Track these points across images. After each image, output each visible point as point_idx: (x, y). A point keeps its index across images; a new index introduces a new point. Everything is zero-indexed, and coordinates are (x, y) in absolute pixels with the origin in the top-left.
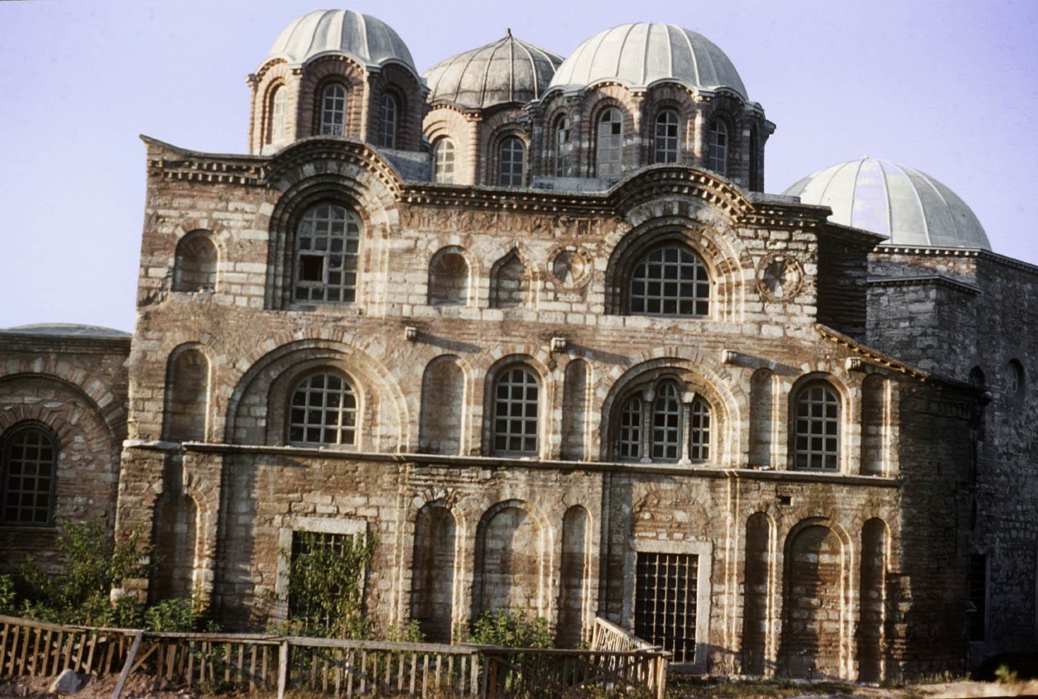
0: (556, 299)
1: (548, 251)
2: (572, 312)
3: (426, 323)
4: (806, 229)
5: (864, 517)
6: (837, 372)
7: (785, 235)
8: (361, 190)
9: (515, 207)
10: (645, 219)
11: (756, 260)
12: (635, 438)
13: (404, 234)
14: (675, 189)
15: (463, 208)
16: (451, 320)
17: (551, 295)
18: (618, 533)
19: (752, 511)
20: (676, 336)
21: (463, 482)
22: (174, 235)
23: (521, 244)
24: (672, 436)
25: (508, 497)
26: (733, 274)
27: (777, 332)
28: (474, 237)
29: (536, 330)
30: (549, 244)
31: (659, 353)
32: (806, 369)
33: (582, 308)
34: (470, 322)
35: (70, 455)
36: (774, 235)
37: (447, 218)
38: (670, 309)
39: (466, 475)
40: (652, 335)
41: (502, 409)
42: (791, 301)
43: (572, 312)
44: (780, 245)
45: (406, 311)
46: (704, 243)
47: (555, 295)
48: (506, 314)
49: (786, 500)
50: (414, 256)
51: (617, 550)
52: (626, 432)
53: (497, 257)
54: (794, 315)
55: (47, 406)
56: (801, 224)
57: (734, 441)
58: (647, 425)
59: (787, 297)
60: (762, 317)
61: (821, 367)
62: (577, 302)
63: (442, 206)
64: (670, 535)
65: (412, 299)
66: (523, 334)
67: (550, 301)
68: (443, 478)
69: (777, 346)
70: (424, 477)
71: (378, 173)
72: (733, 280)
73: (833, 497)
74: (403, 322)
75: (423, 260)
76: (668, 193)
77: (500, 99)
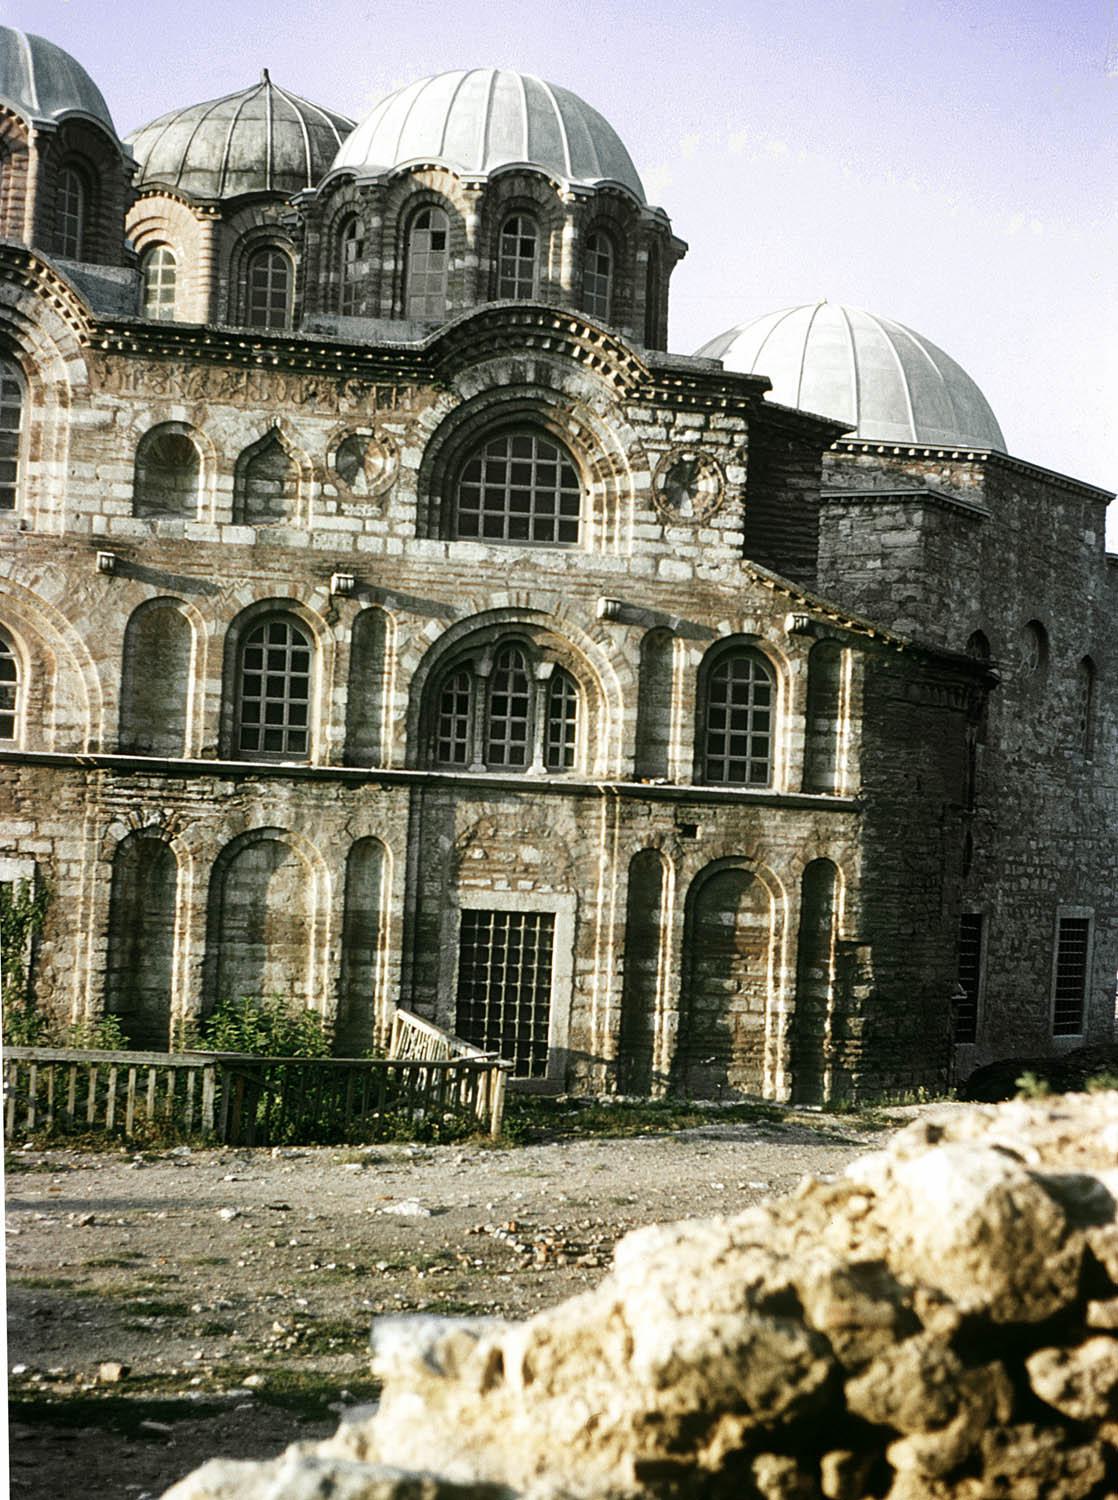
0: (340, 512)
1: (327, 433)
2: (364, 533)
3: (131, 546)
4: (731, 411)
5: (806, 857)
6: (772, 634)
7: (697, 420)
8: (24, 326)
9: (275, 362)
10: (481, 388)
11: (653, 458)
12: (461, 733)
13: (97, 401)
14: (530, 343)
15: (192, 361)
16: (171, 542)
17: (332, 506)
18: (432, 879)
19: (638, 848)
20: (528, 575)
21: (188, 800)
23: (285, 422)
24: (519, 731)
25: (261, 824)
26: (617, 479)
27: (683, 572)
28: (210, 409)
30: (329, 424)
31: (500, 600)
32: (725, 629)
33: (381, 527)
34: (202, 545)
36: (682, 419)
37: (166, 378)
38: (518, 531)
39: (195, 788)
40: (489, 573)
41: (253, 685)
42: (706, 524)
43: (364, 533)
44: (690, 436)
45: (99, 525)
46: (574, 429)
47: (339, 505)
48: (260, 535)
49: (690, 831)
50: (112, 436)
51: (431, 907)
52: (447, 723)
53: (246, 443)
54: (709, 545)
56: (724, 404)
57: (613, 739)
58: (479, 713)
59: (699, 517)
60: (661, 548)
61: (749, 626)
62: (373, 518)
63: (157, 356)
64: (512, 884)
65: (108, 508)
66: (286, 566)
67: (330, 515)
68: (157, 793)
69: (681, 594)
70: (126, 792)
71: (52, 299)
72: (618, 489)
73: (761, 827)
74: (93, 543)
75: (126, 443)
76: (519, 348)
77: (251, 186)
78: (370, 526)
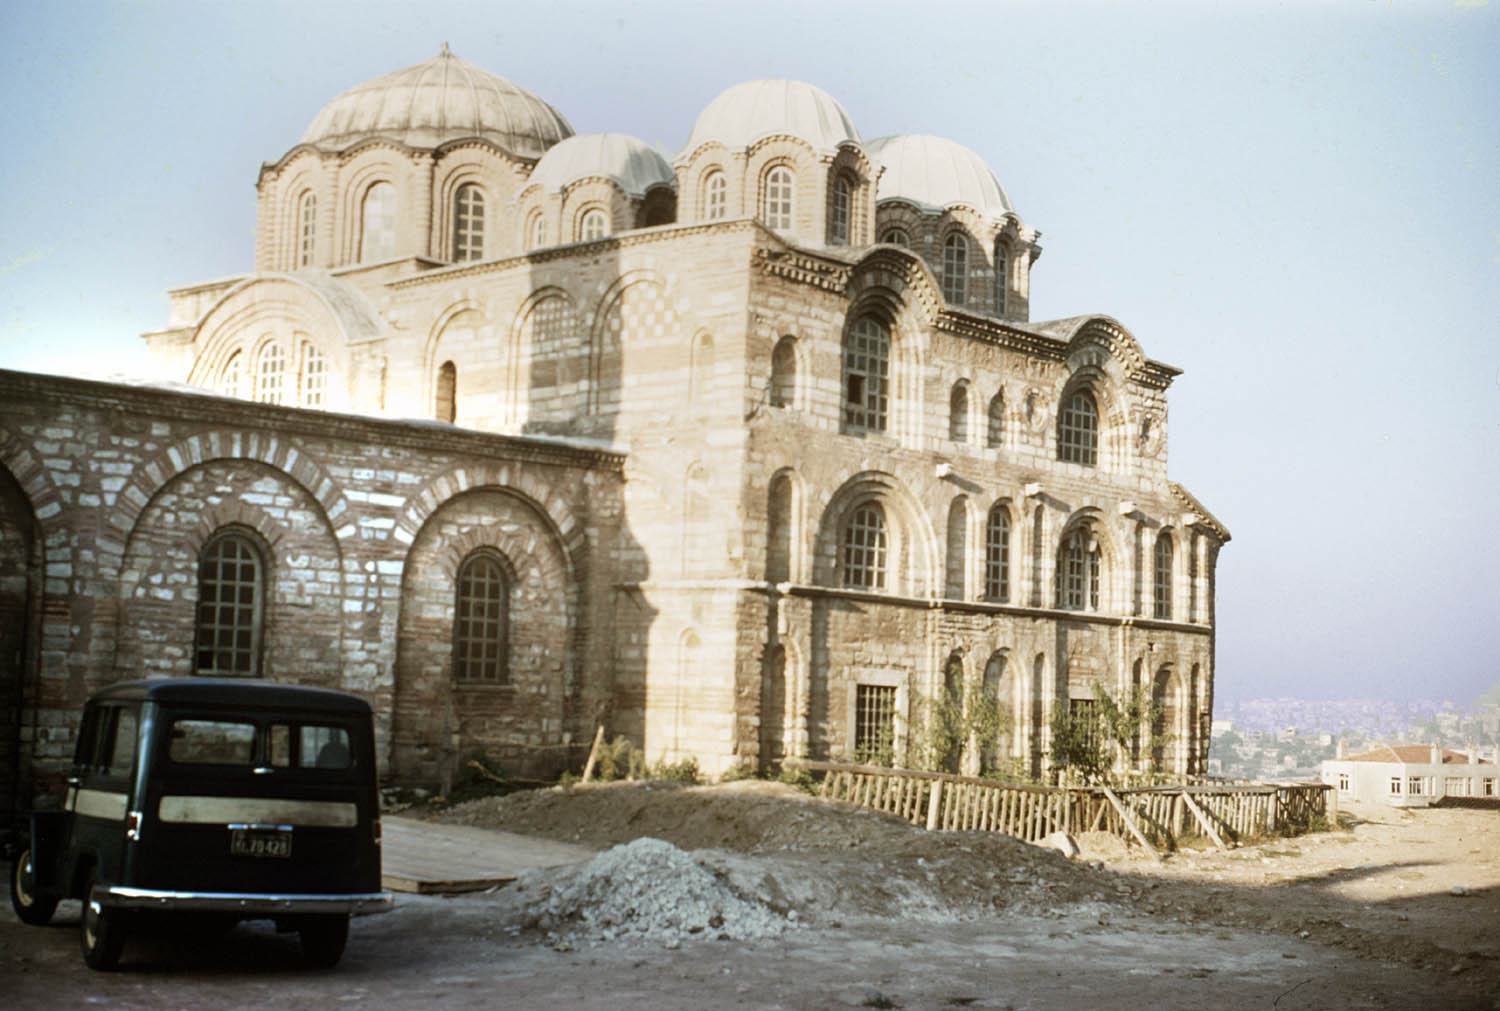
6: (1178, 527)
8: (901, 307)
22: (769, 339)
26: (1122, 428)
29: (1017, 473)
35: (526, 593)
46: (1105, 395)
55: (505, 528)
57: (1124, 590)
71: (919, 291)
72: (1122, 433)
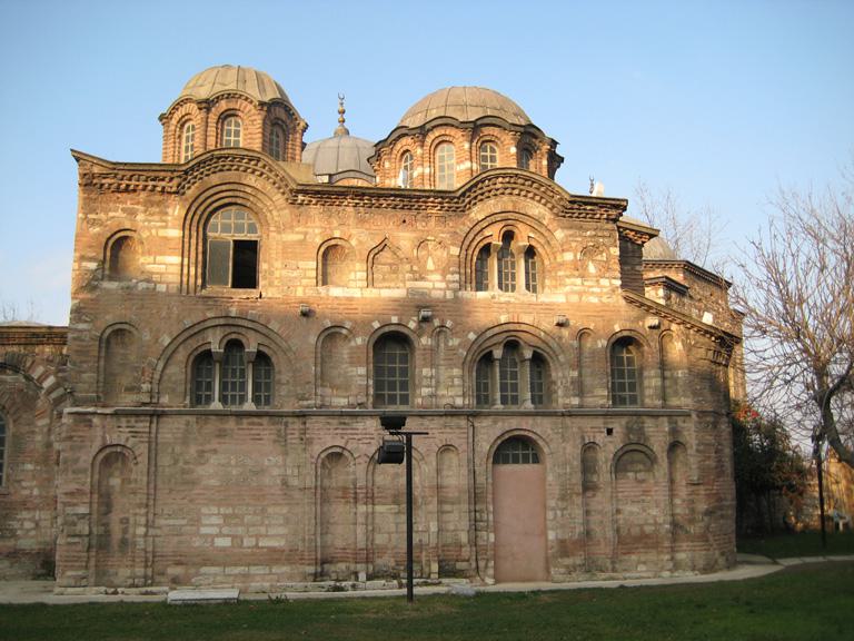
30: (414, 235)
43: (434, 288)
49: (610, 432)
78: (438, 285)
